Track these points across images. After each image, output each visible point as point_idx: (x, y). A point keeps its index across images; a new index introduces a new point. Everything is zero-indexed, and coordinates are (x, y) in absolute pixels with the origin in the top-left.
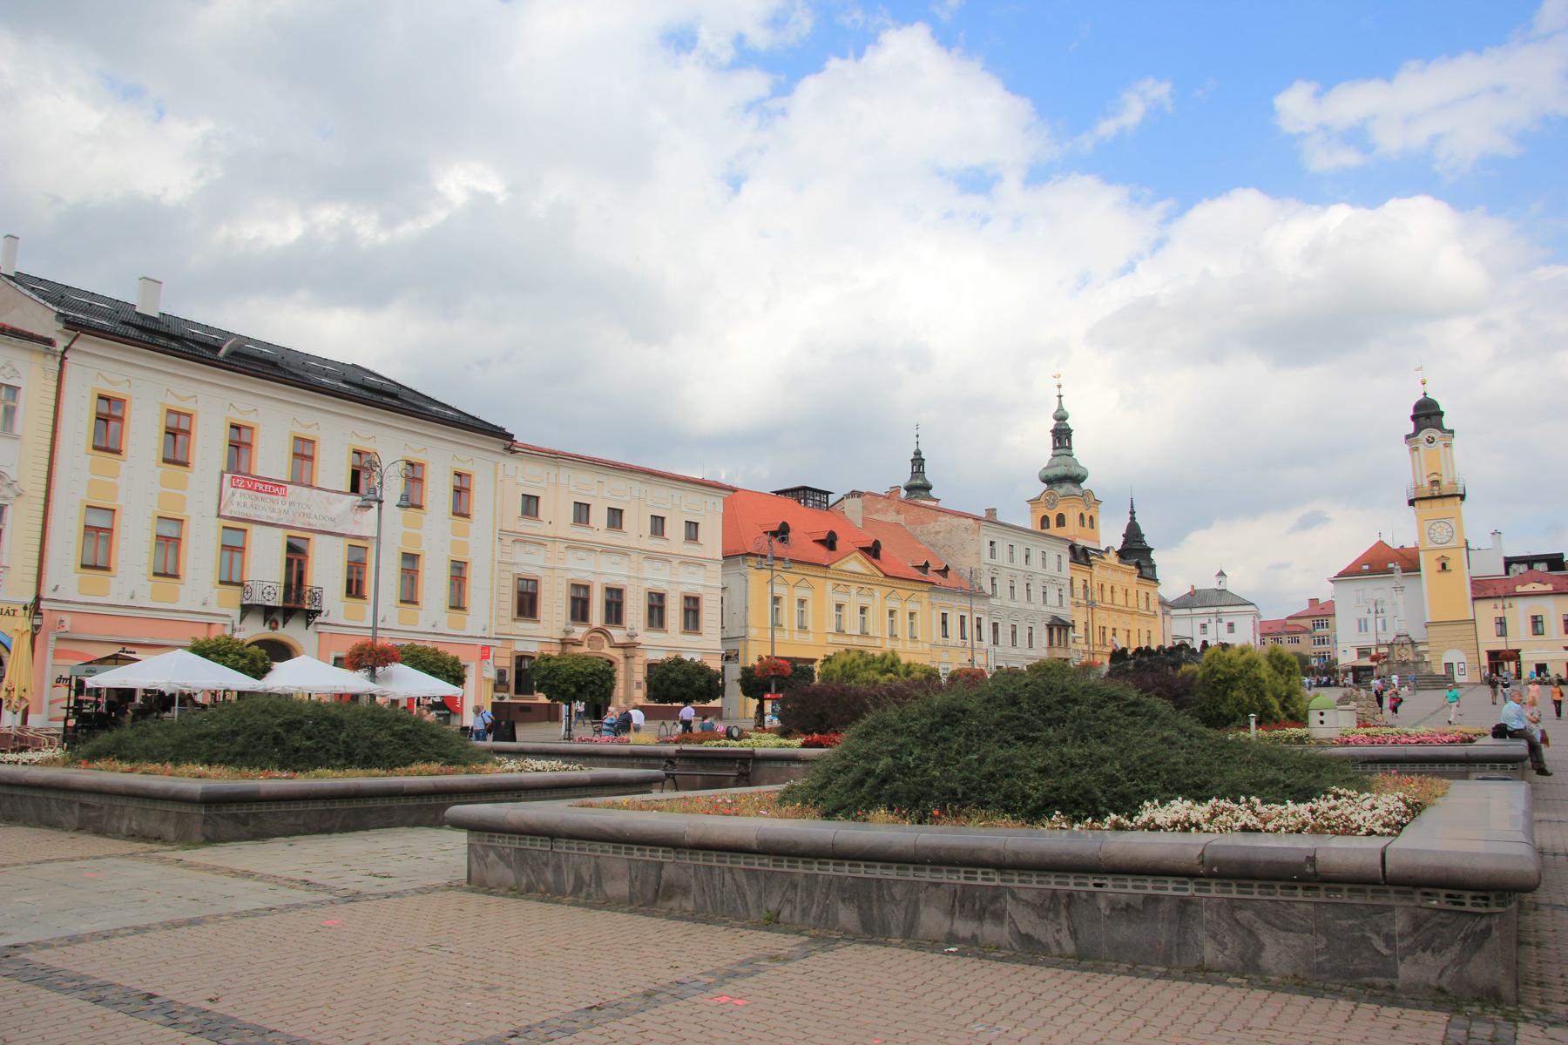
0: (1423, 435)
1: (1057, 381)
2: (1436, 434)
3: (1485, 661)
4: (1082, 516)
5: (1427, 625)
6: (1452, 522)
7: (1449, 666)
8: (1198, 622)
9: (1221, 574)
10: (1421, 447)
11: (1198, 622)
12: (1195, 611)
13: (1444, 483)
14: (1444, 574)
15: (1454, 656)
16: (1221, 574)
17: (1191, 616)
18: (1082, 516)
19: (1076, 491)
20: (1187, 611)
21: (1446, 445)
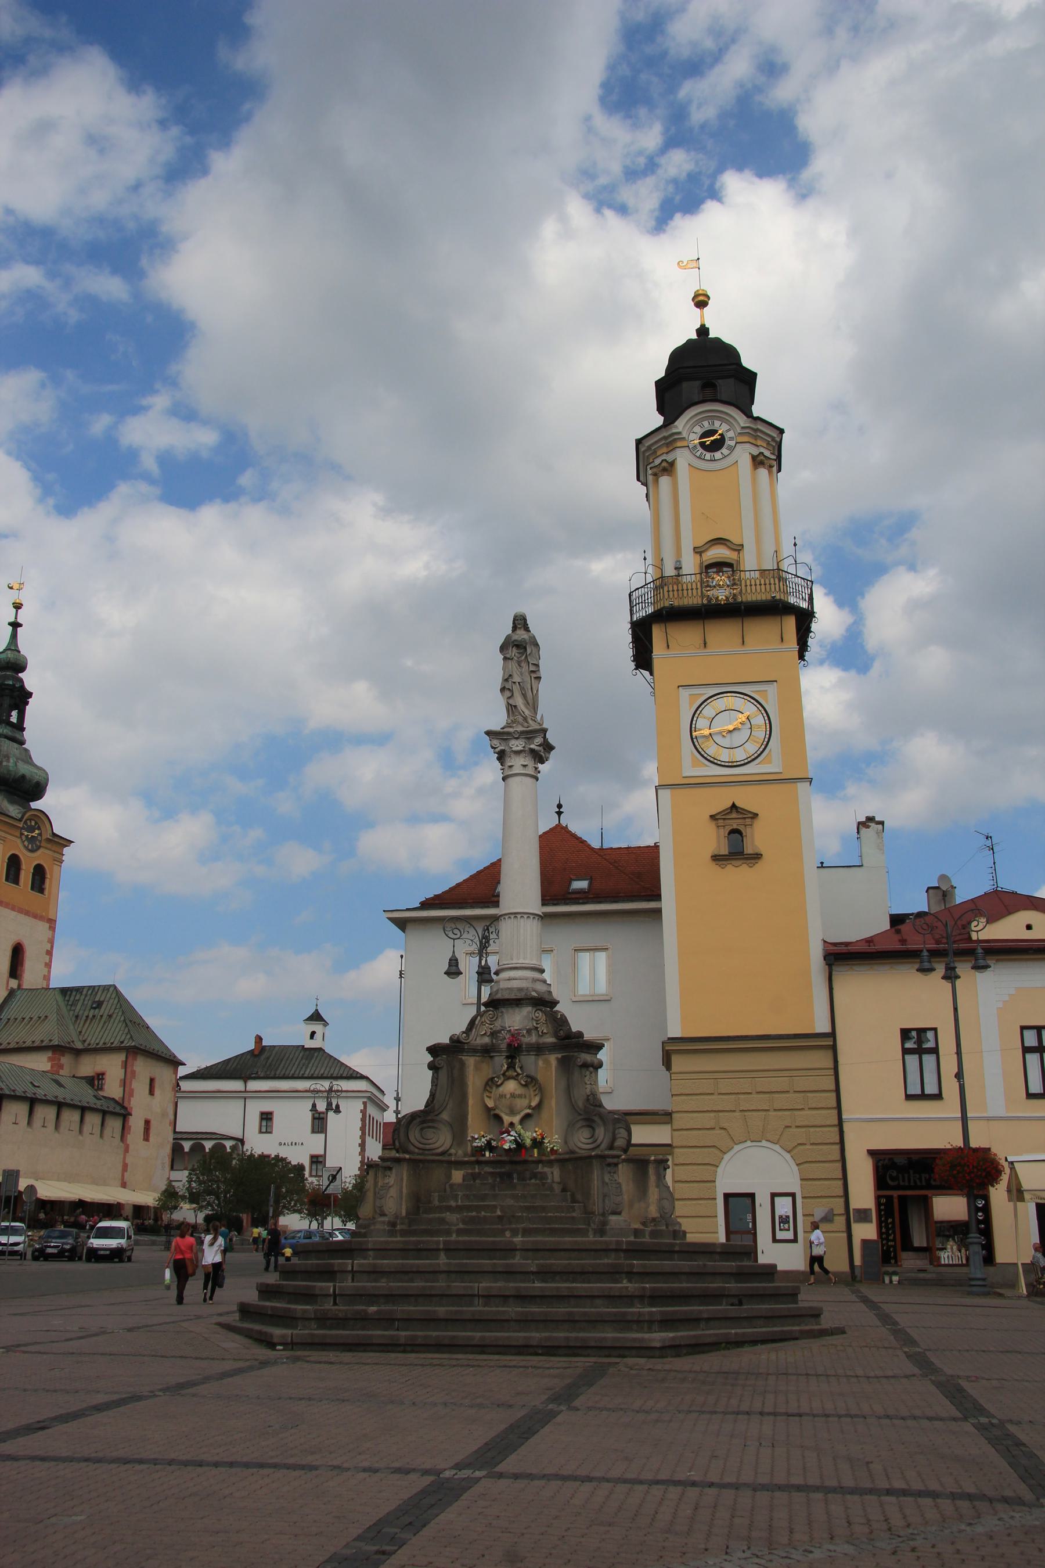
0: (689, 426)
1: (13, 596)
2: (729, 423)
3: (863, 1193)
4: (14, 863)
5: (671, 1051)
6: (771, 697)
7: (741, 1204)
8: (255, 1108)
9: (316, 1017)
10: (683, 459)
11: (255, 1108)
12: (254, 1085)
13: (749, 561)
14: (737, 874)
15: (759, 1169)
16: (316, 1017)
17: (245, 1096)
18: (14, 863)
19: (14, 810)
20: (236, 1085)
21: (758, 461)
